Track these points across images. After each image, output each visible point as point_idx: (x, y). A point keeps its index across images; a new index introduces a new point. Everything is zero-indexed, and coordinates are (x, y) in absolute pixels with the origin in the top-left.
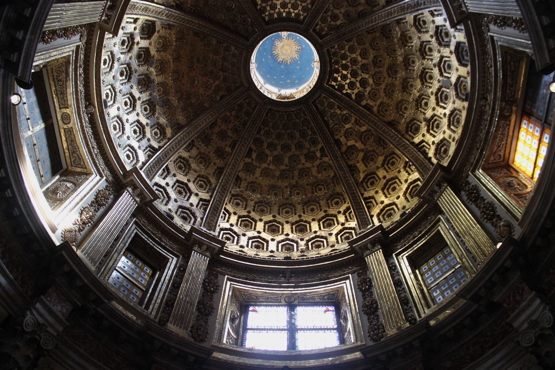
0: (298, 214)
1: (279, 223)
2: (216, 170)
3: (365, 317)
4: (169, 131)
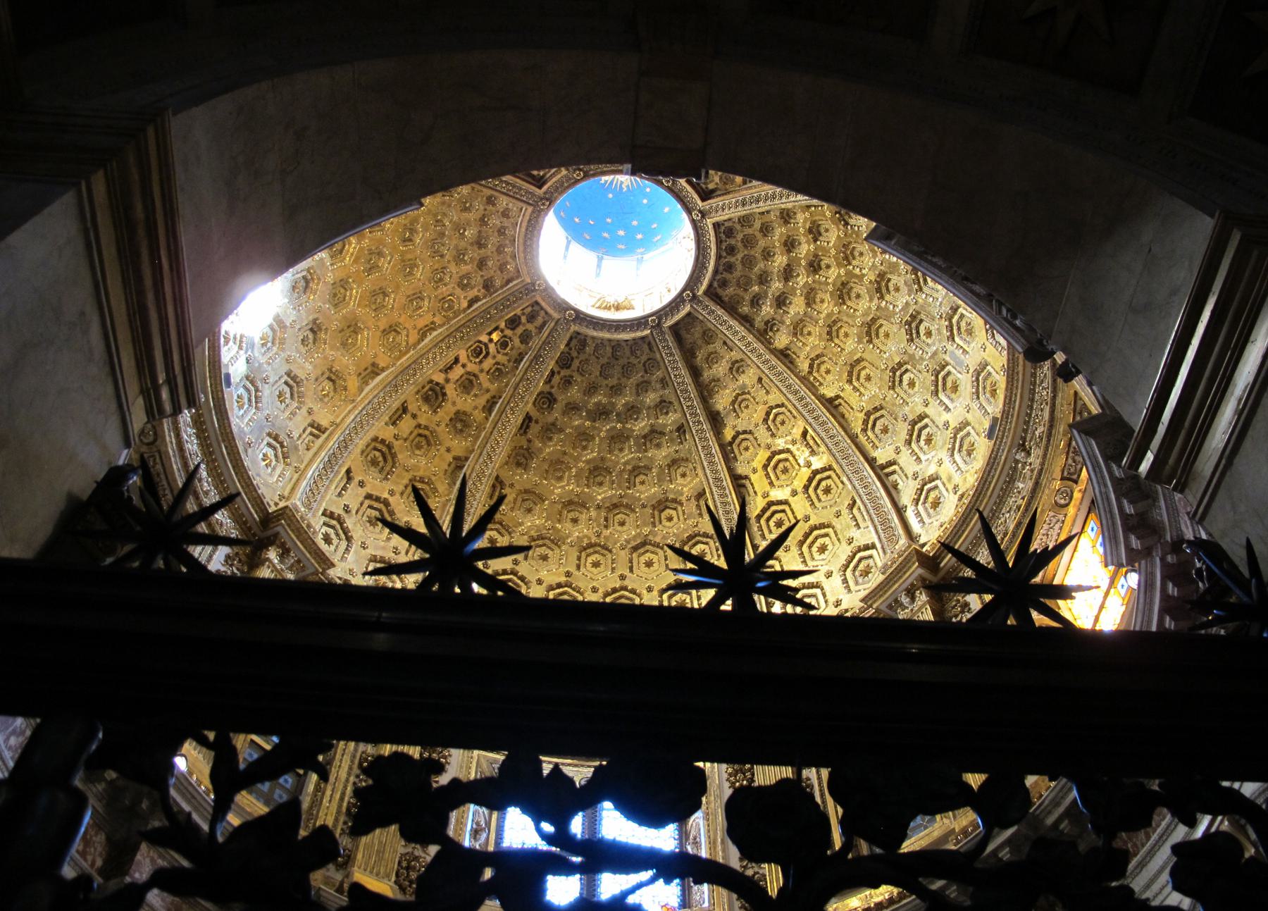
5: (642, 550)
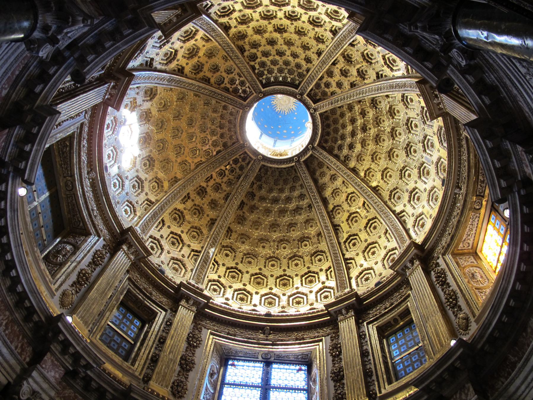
0: (283, 268)
1: (264, 276)
2: (208, 222)
3: (332, 384)
4: (166, 185)
5: (293, 259)
